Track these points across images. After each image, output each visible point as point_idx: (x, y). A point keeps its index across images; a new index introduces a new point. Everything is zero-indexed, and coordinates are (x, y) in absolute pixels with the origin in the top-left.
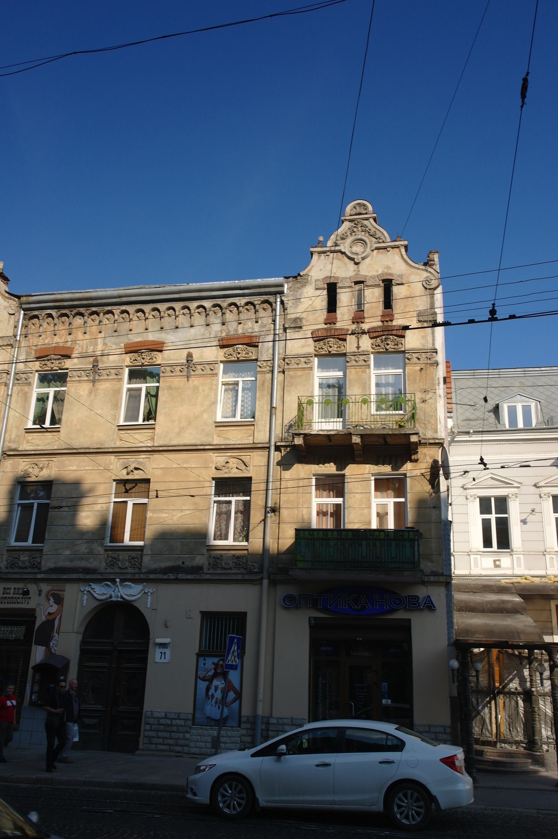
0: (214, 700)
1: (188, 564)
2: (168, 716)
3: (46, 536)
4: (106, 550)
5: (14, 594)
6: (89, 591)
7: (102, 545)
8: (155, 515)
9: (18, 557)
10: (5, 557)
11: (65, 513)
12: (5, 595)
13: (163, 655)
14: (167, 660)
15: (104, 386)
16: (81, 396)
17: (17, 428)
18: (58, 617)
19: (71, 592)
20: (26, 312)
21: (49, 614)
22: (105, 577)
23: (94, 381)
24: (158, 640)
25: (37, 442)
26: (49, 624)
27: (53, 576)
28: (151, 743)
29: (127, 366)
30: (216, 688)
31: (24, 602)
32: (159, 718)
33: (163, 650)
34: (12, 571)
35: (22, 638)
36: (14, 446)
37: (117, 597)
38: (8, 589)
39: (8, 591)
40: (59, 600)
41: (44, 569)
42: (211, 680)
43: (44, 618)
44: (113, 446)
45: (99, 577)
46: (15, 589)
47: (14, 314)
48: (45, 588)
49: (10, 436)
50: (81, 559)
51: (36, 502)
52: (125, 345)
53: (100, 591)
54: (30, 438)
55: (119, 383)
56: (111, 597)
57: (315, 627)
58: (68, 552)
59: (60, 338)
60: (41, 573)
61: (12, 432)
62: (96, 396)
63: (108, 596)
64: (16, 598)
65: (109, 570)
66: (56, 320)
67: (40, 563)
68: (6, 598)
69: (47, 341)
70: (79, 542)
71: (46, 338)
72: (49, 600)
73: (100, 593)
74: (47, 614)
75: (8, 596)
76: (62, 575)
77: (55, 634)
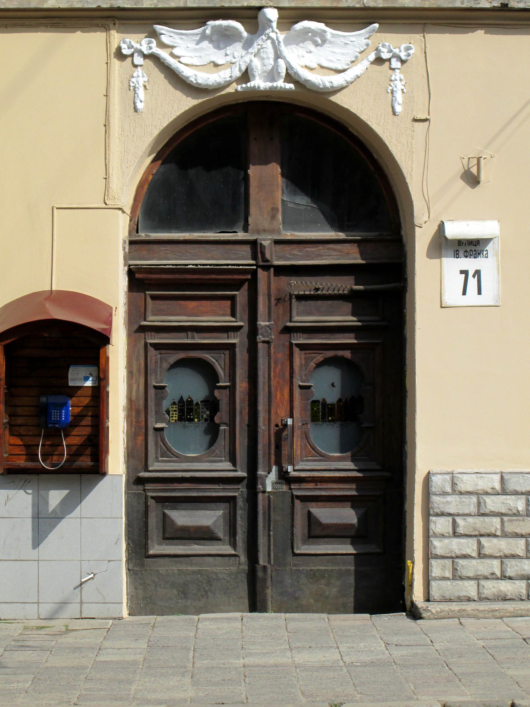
2: (512, 486)
13: (472, 282)
14: (488, 296)
24: (453, 230)
28: (456, 576)
32: (480, 494)
33: (470, 264)
56: (246, 76)
73: (196, 61)
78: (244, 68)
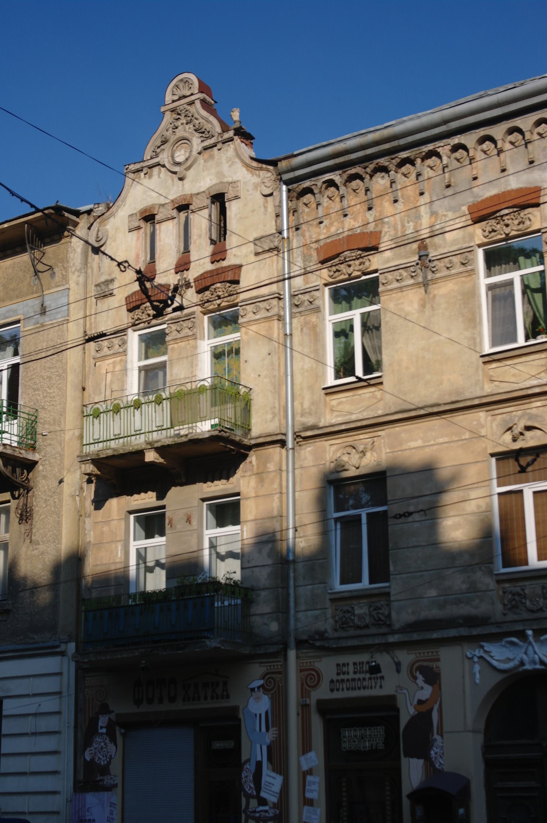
3: (392, 568)
4: (498, 582)
5: (355, 673)
6: (481, 657)
7: (490, 572)
9: (350, 609)
10: (329, 612)
11: (416, 525)
12: (341, 677)
15: (445, 290)
17: (311, 388)
18: (436, 707)
19: (450, 660)
20: (290, 187)
21: (420, 702)
22: (505, 629)
23: (425, 284)
25: (347, 407)
26: (423, 719)
27: (415, 636)
29: (479, 246)
31: (373, 684)
34: (344, 634)
35: (381, 746)
36: (310, 421)
37: (534, 662)
38: (344, 665)
39: (345, 669)
40: (432, 677)
41: (397, 626)
43: (412, 711)
44: (479, 394)
45: (494, 630)
46: (355, 664)
47: (271, 195)
48: (406, 657)
49: (302, 404)
51: (363, 513)
52: (469, 208)
53: (502, 656)
54: (334, 403)
55: (469, 278)
56: (522, 663)
58: (433, 593)
59: (355, 219)
60: (393, 632)
61: (303, 398)
62: (433, 308)
63: (516, 662)
64: (359, 679)
65: (511, 617)
66: (342, 189)
67: (389, 616)
68: (343, 681)
69: (333, 230)
70: (450, 571)
71: (331, 224)
72: (415, 678)
73: (501, 658)
74: (415, 702)
76: (429, 633)
77: (436, 736)
78: (520, 660)
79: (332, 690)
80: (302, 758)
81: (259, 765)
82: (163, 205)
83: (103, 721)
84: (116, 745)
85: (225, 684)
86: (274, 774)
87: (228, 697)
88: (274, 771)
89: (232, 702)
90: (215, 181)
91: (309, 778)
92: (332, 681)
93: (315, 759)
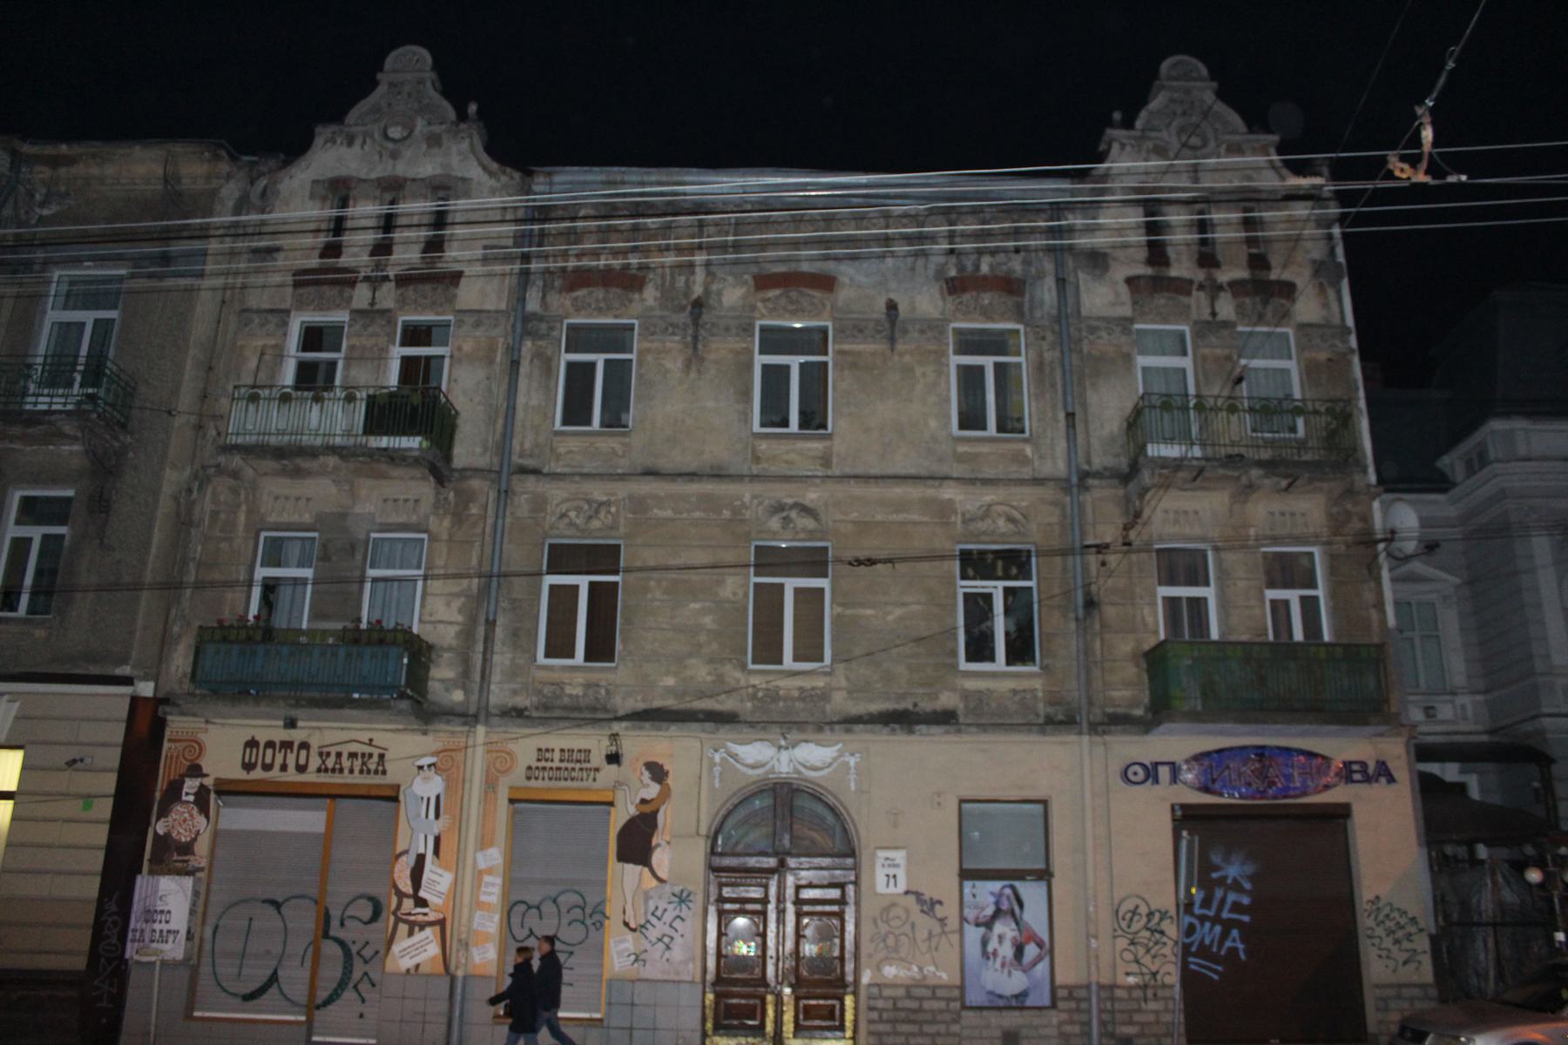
0: (999, 960)
1: (926, 706)
7: (743, 667)
8: (848, 612)
16: (667, 371)
21: (643, 801)
30: (1001, 938)
39: (548, 755)
41: (621, 713)
42: (988, 924)
43: (633, 811)
46: (562, 750)
49: (522, 444)
50: (701, 695)
57: (1186, 817)
62: (699, 371)
68: (544, 768)
70: (693, 661)
75: (549, 764)
79: (529, 778)
80: (479, 856)
81: (421, 859)
82: (365, 181)
83: (191, 785)
84: (207, 817)
85: (382, 756)
86: (440, 871)
87: (384, 772)
88: (440, 866)
89: (390, 779)
90: (438, 171)
91: (487, 878)
92: (529, 768)
93: (494, 856)
